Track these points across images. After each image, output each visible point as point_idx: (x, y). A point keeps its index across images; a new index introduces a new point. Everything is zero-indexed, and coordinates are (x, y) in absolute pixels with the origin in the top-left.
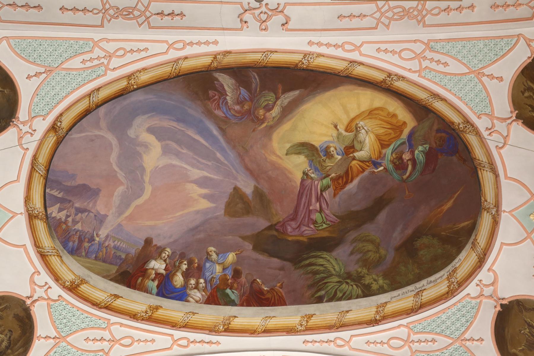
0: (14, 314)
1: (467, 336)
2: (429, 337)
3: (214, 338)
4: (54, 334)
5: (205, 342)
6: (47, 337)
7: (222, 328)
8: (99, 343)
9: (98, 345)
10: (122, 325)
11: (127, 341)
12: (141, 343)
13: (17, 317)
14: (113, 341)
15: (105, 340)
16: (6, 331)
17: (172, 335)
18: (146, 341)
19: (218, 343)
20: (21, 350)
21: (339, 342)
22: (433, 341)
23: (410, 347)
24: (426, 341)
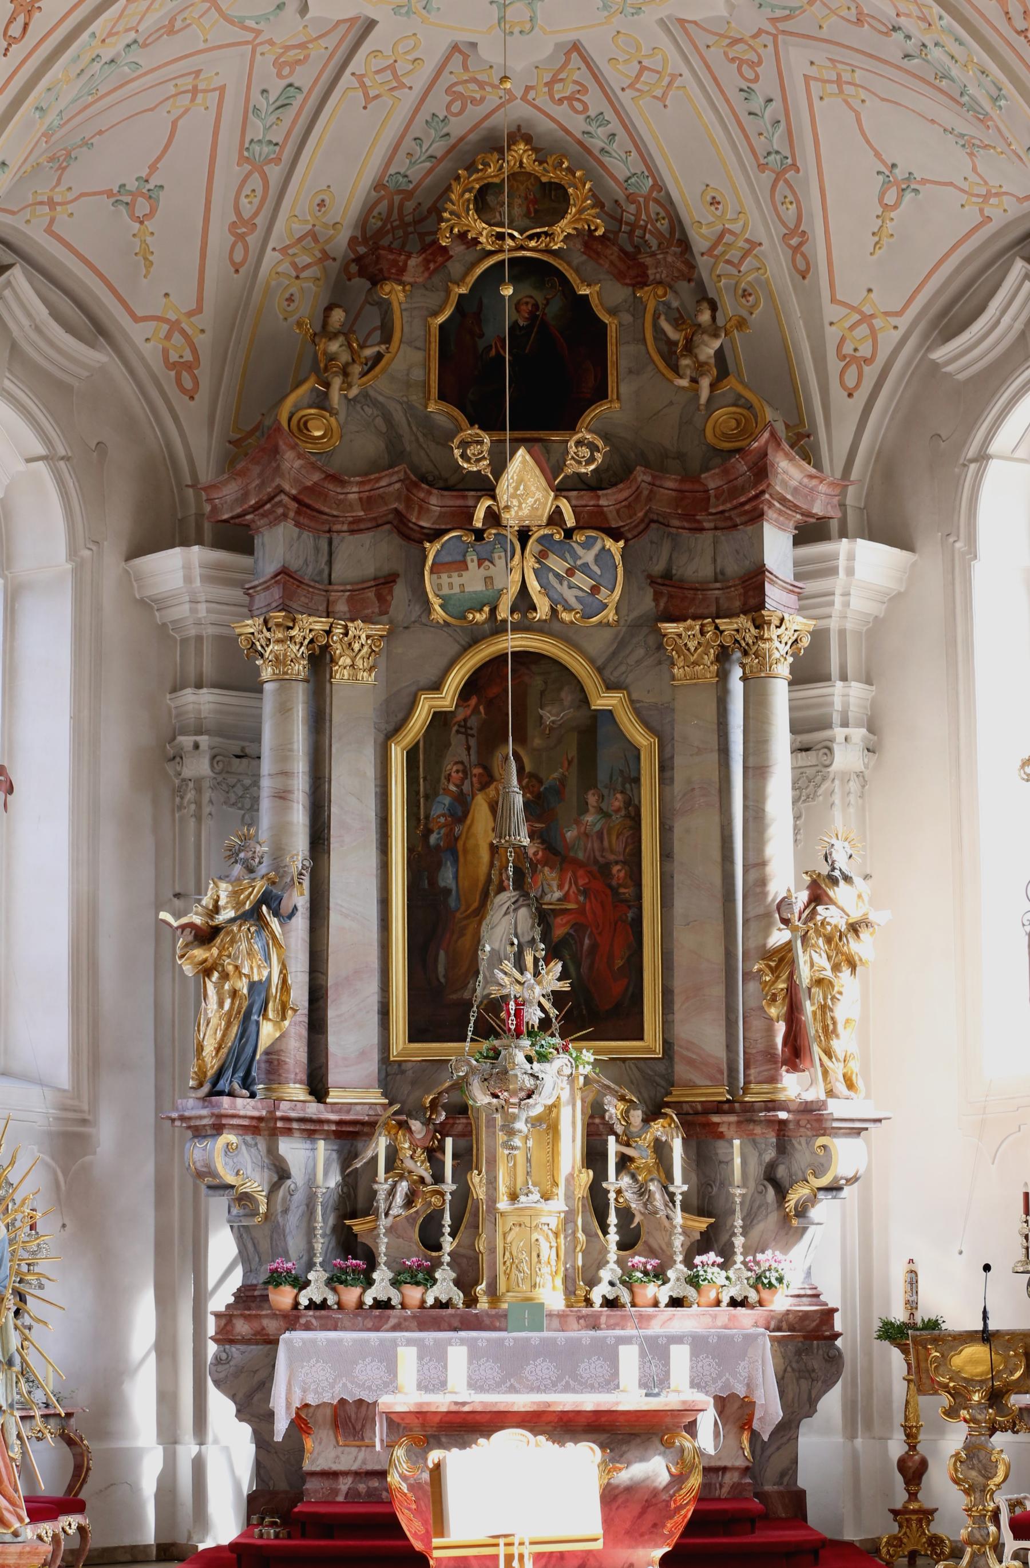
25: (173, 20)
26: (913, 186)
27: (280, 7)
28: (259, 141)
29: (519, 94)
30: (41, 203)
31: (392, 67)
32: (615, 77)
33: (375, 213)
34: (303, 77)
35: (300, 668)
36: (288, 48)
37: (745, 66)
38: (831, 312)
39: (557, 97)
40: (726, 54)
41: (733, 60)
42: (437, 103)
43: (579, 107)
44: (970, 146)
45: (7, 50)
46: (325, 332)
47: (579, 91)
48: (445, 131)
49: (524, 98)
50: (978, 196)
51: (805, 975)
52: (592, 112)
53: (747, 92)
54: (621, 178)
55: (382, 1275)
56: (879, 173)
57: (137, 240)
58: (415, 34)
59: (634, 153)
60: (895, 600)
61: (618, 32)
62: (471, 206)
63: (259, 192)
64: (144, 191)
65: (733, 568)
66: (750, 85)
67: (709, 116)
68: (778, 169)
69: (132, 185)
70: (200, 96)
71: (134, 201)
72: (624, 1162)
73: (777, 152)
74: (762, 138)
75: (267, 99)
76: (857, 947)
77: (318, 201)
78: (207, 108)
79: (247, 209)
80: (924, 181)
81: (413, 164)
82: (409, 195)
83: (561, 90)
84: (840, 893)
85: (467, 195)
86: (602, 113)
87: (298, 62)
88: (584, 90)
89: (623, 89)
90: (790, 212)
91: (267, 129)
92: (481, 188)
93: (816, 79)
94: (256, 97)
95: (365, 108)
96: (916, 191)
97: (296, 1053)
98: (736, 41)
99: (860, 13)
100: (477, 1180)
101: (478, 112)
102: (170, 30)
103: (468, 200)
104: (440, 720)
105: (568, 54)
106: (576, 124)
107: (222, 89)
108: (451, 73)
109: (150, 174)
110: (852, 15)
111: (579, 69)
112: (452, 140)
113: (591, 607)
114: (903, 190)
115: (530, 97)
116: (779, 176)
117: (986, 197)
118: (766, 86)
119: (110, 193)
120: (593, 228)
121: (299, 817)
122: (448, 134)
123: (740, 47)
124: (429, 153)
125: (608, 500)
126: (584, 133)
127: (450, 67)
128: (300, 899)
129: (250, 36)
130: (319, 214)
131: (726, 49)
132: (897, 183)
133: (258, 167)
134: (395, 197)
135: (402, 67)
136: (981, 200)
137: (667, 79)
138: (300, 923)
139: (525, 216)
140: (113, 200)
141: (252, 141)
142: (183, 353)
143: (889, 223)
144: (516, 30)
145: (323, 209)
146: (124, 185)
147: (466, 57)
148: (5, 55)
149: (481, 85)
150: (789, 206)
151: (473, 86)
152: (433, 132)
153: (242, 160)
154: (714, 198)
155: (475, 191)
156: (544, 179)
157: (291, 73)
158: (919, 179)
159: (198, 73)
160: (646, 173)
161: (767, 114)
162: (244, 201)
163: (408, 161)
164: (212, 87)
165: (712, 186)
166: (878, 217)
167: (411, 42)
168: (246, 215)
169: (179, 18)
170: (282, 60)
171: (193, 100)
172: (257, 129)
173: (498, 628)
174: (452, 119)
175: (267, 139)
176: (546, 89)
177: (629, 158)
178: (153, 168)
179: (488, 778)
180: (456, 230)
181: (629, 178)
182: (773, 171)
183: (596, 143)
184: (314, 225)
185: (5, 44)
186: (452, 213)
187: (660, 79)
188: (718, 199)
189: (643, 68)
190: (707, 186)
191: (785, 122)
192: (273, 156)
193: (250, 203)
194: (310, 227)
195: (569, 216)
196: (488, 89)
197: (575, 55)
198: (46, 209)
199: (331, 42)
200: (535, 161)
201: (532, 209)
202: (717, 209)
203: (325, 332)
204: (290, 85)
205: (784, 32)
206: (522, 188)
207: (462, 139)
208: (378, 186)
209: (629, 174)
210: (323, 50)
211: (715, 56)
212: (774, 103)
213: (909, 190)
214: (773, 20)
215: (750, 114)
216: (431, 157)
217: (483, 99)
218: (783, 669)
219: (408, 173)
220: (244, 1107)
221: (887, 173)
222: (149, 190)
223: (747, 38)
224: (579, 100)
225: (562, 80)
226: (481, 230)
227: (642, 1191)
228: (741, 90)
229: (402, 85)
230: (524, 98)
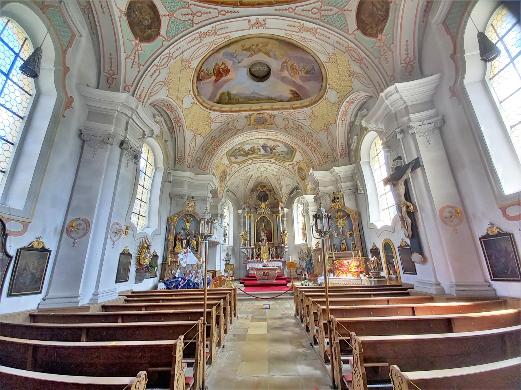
0: (147, 5)
1: (346, 8)
2: (329, 8)
3: (236, 9)
4: (167, 13)
5: (232, 12)
6: (165, 15)
7: (239, 3)
8: (187, 16)
9: (187, 17)
10: (194, 5)
11: (199, 14)
12: (205, 14)
13: (148, 5)
14: (193, 14)
15: (189, 14)
16: (148, 15)
17: (217, 9)
18: (207, 13)
19: (238, 12)
20: (157, 23)
21: (291, 10)
22: (331, 10)
23: (320, 13)
24: (328, 10)
35: (249, 218)
38: (283, 193)
42: (257, 180)
44: (292, 182)
46: (250, 195)
51: (283, 237)
55: (255, 259)
60: (288, 212)
65: (277, 210)
72: (271, 251)
76: (287, 235)
84: (285, 232)
97: (249, 243)
100: (261, 252)
102: (239, 175)
104: (258, 221)
106: (266, 182)
113: (268, 213)
118: (279, 179)
121: (249, 227)
125: (269, 206)
128: (249, 233)
138: (249, 235)
142: (241, 197)
172: (245, 182)
173: (262, 214)
179: (261, 225)
203: (250, 195)
218: (281, 217)
220: (245, 247)
226: (260, 189)
227: (273, 253)
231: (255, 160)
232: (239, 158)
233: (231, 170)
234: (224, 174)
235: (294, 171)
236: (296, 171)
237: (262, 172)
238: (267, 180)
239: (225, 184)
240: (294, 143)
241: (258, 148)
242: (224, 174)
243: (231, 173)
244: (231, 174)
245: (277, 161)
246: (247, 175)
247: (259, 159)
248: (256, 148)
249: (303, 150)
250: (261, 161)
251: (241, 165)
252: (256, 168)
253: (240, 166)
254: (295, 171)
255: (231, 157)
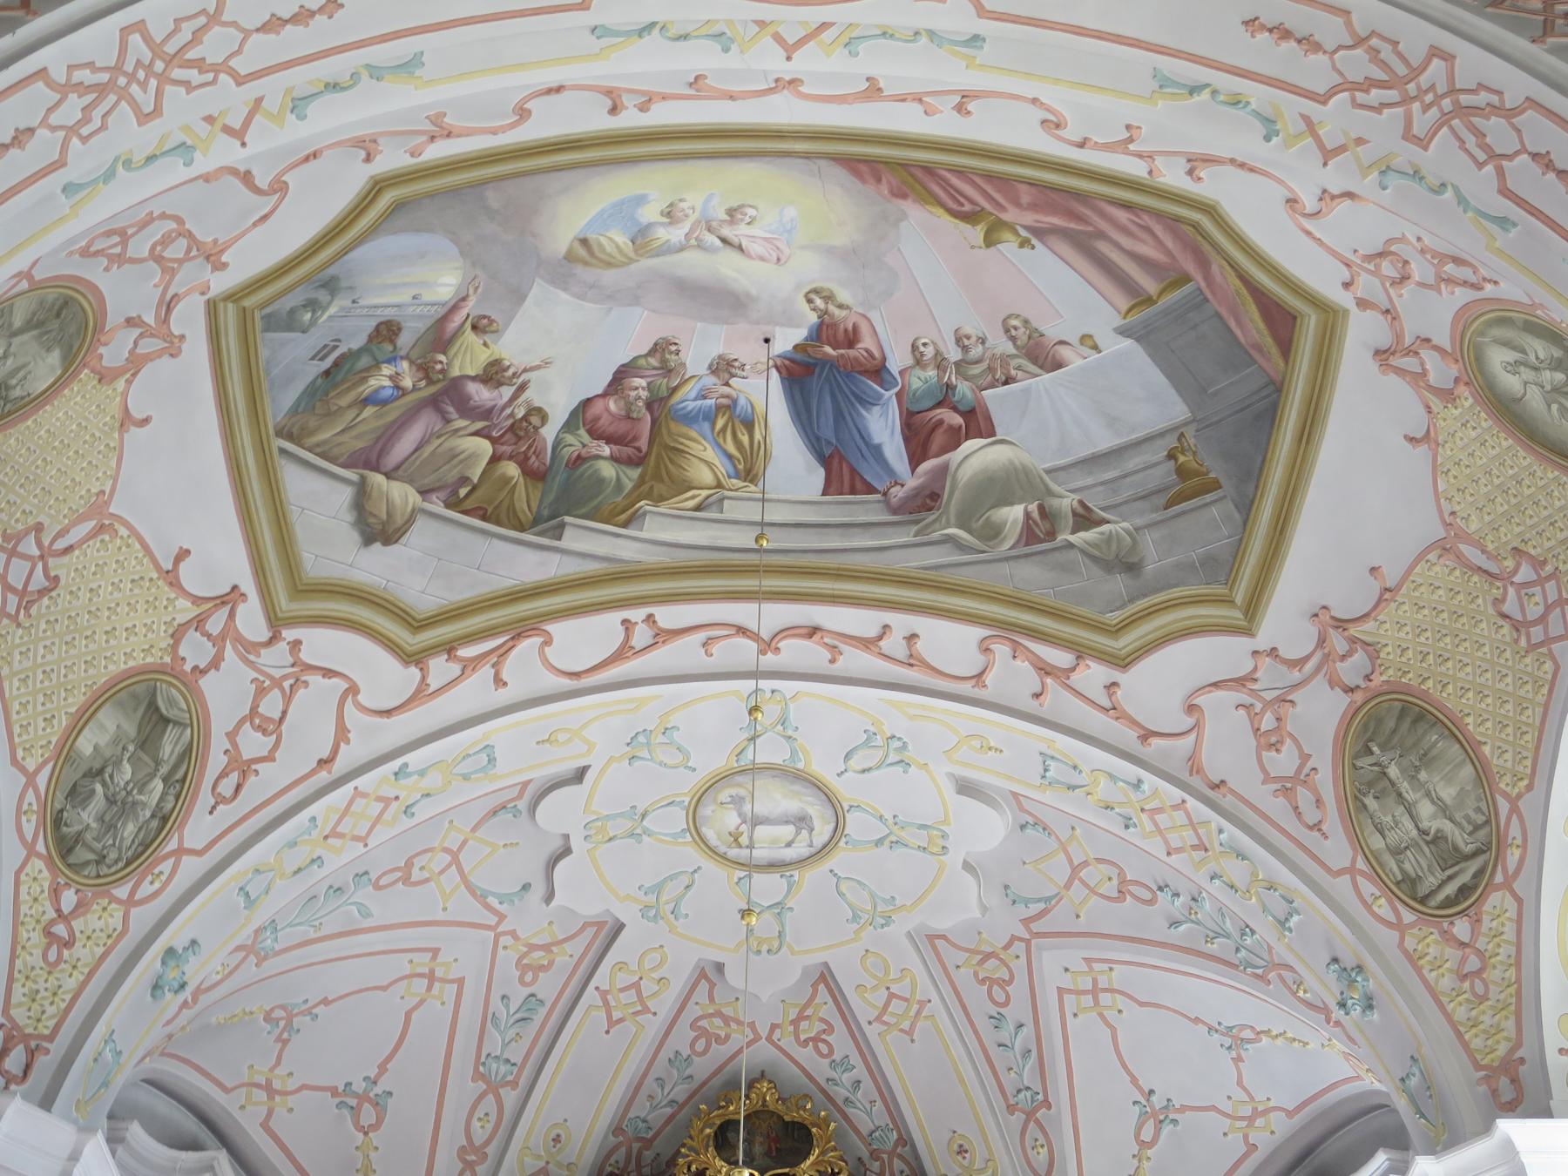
25: (409, 864)
26: (1171, 1116)
27: (526, 887)
28: (496, 1057)
29: (764, 1032)
30: (258, 1086)
31: (636, 986)
32: (863, 1009)
33: (612, 1161)
34: (547, 987)
36: (533, 947)
37: (995, 987)
39: (803, 1037)
40: (976, 974)
41: (983, 981)
42: (682, 1039)
43: (824, 1048)
45: (214, 808)
47: (825, 1030)
48: (688, 1072)
49: (769, 1039)
50: (1242, 1118)
52: (837, 1056)
53: (997, 1020)
54: (865, 1132)
56: (1135, 1103)
57: (359, 1154)
58: (661, 946)
59: (879, 1103)
61: (867, 951)
62: (711, 1143)
63: (493, 1117)
64: (371, 1095)
66: (1001, 1010)
67: (957, 1050)
68: (1028, 1108)
69: (359, 1086)
70: (437, 985)
71: (360, 1106)
73: (1028, 1088)
74: (1012, 1074)
75: (507, 1007)
77: (553, 1135)
78: (443, 1004)
79: (480, 1133)
80: (1184, 1109)
81: (654, 1108)
82: (648, 1143)
83: (809, 1029)
85: (708, 1131)
86: (847, 1057)
87: (542, 968)
88: (830, 1029)
89: (870, 1023)
90: (1041, 1156)
91: (505, 1045)
92: (721, 1126)
93: (1070, 991)
94: (496, 1004)
95: (607, 1032)
96: (1174, 1122)
98: (987, 956)
99: (1123, 882)
101: (720, 1052)
103: (708, 1136)
105: (815, 986)
106: (821, 1069)
107: (460, 982)
108: (697, 1003)
109: (379, 1075)
110: (1110, 888)
111: (826, 1003)
112: (695, 1085)
114: (1161, 1122)
115: (775, 1038)
116: (1030, 1115)
117: (1250, 1120)
118: (1018, 1010)
119: (334, 1091)
120: (836, 1171)
122: (690, 1077)
123: (992, 962)
124: (670, 1097)
126: (828, 1080)
127: (695, 998)
129: (493, 920)
130: (554, 1150)
131: (977, 968)
132: (1154, 1114)
133: (493, 1088)
134: (634, 1145)
135: (648, 987)
136: (1244, 1124)
137: (915, 1007)
139: (766, 1154)
140: (337, 1100)
141: (489, 1055)
143: (1146, 1164)
144: (765, 948)
145: (558, 1146)
146: (350, 1084)
147: (712, 985)
148: (211, 813)
149: (726, 1020)
150: (1041, 1150)
151: (717, 1021)
152: (675, 1072)
153: (478, 1076)
154: (961, 1146)
155: (715, 1128)
156: (787, 1118)
157: (535, 979)
158: (1177, 1106)
159: (435, 952)
160: (891, 1126)
161: (1018, 1043)
162: (476, 1124)
163: (648, 1104)
164: (451, 977)
165: (959, 1132)
166: (1134, 1156)
167: (657, 956)
168: (478, 1142)
169: (418, 862)
170: (525, 961)
171: (429, 988)
174: (696, 1059)
175: (505, 1057)
176: (791, 1028)
177: (874, 1109)
178: (383, 1068)
180: (693, 1168)
181: (873, 1132)
182: (1024, 1112)
183: (840, 1093)
184: (548, 1163)
185: (212, 801)
186: (691, 1149)
187: (908, 1009)
188: (966, 1147)
189: (892, 996)
190: (955, 1132)
191: (1037, 1052)
192: (510, 1078)
193: (483, 1127)
194: (543, 1164)
195: (812, 1158)
196: (734, 1025)
197: (822, 987)
198: (263, 1096)
199: (576, 948)
200: (778, 1100)
201: (774, 1148)
202: (964, 1158)
204: (533, 995)
205: (1039, 935)
206: (764, 1125)
207: (704, 1084)
208: (617, 1130)
209: (873, 1128)
210: (567, 958)
211: (964, 977)
212: (1025, 1029)
213: (1167, 1121)
214: (1026, 922)
215: (1000, 1045)
216: (673, 1101)
217: (728, 1037)
219: (649, 1118)
221: (1145, 1103)
222: (376, 1095)
223: (998, 951)
224: (824, 1041)
225: (808, 1017)
228: (991, 1017)
229: (646, 1010)
230: (769, 1039)
231: (668, 616)
232: (422, 535)
233: (271, 706)
234: (147, 741)
235: (1286, 787)
236: (1325, 779)
237: (768, 887)
238: (840, 1042)
239: (142, 918)
240: (1314, 71)
241: (728, 407)
242: (147, 741)
243: (268, 779)
244: (256, 792)
245: (1001, 650)
246: (532, 921)
247: (740, 612)
248: (687, 399)
249: (1494, 127)
250: (768, 645)
251: (441, 668)
252: (687, 785)
253: (421, 694)
254: (1302, 777)
255: (298, 483)
